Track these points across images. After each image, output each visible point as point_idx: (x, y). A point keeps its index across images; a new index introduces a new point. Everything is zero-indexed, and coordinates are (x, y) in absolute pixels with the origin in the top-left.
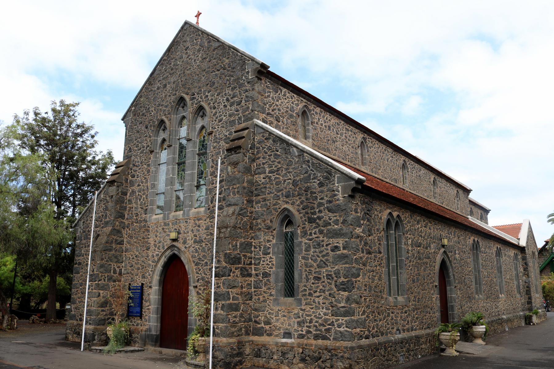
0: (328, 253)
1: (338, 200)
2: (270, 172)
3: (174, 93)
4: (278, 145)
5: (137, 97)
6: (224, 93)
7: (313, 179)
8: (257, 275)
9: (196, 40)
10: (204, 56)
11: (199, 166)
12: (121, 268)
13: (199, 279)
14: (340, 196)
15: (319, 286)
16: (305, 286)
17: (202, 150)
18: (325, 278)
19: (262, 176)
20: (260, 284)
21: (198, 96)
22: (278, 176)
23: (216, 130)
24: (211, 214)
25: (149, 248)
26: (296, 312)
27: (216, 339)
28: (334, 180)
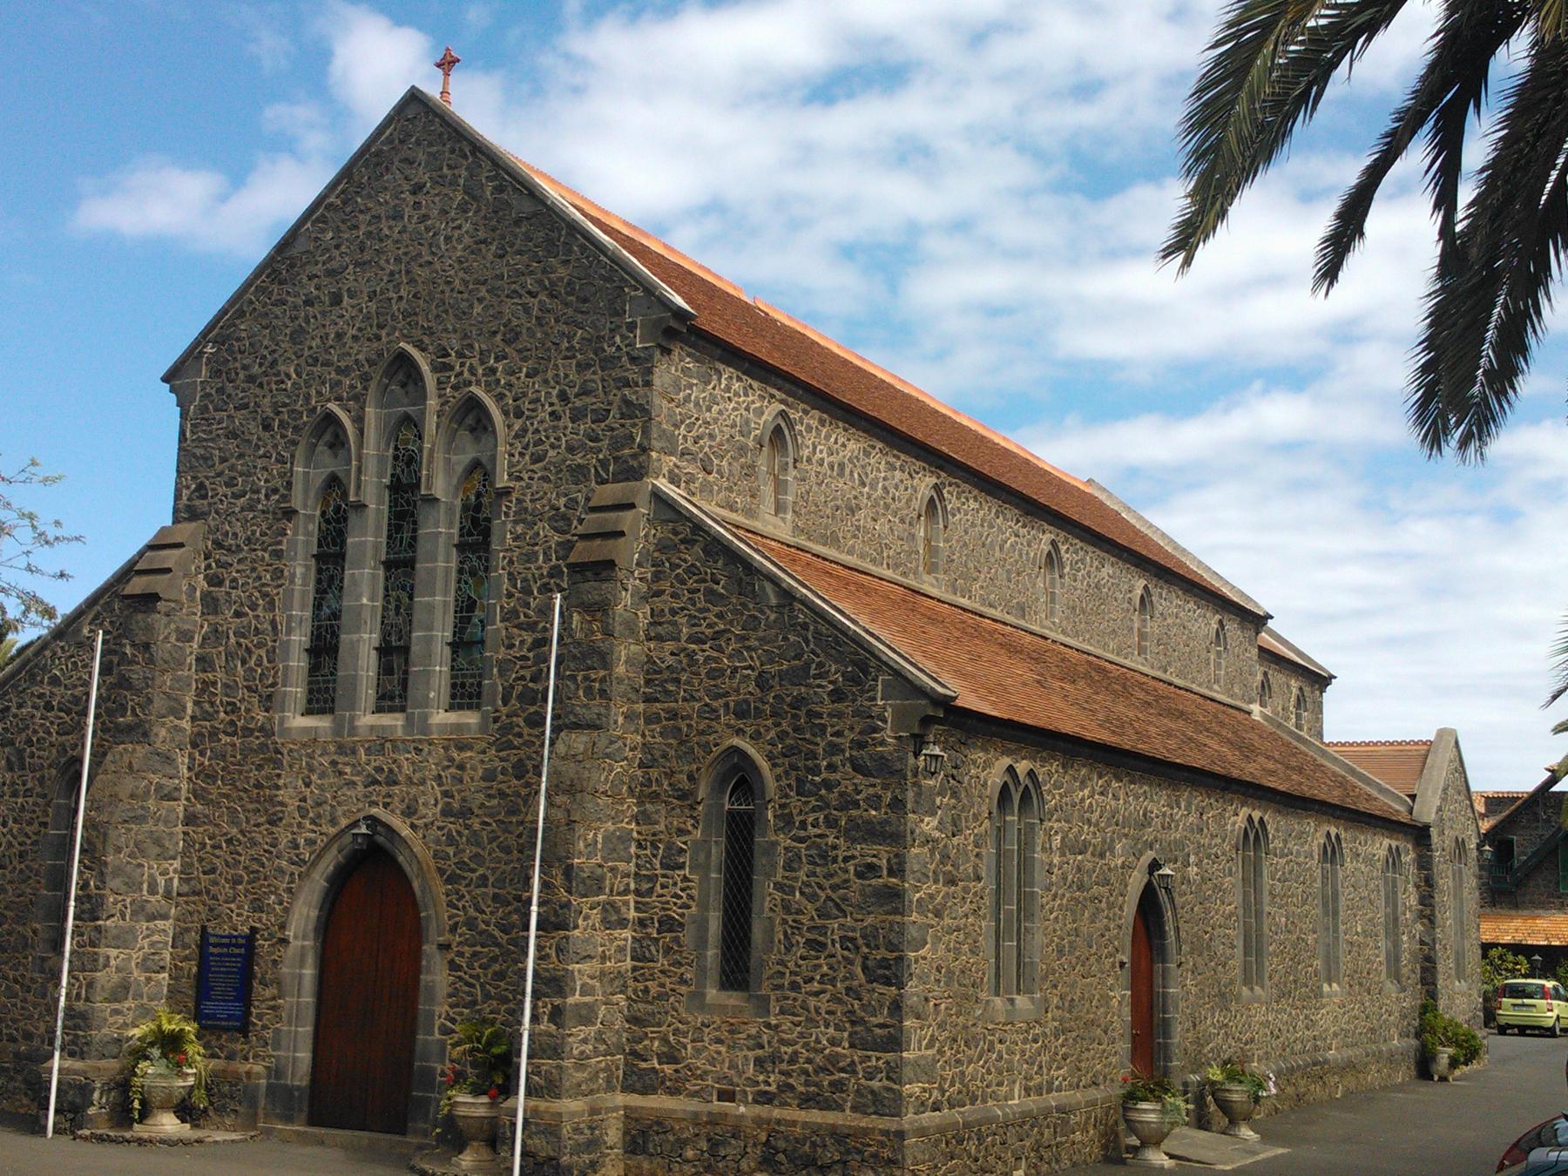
0: (847, 881)
1: (883, 743)
2: (691, 639)
3: (370, 332)
4: (720, 563)
5: (223, 312)
6: (550, 374)
7: (815, 677)
8: (642, 923)
9: (450, 167)
10: (482, 235)
11: (459, 582)
12: (172, 875)
13: (457, 923)
14: (888, 734)
15: (820, 966)
16: (782, 963)
17: (470, 534)
18: (838, 945)
19: (670, 646)
20: (653, 948)
21: (462, 365)
22: (715, 654)
23: (523, 484)
24: (502, 736)
25: (281, 819)
26: (753, 1031)
27: (533, 1103)
28: (873, 688)
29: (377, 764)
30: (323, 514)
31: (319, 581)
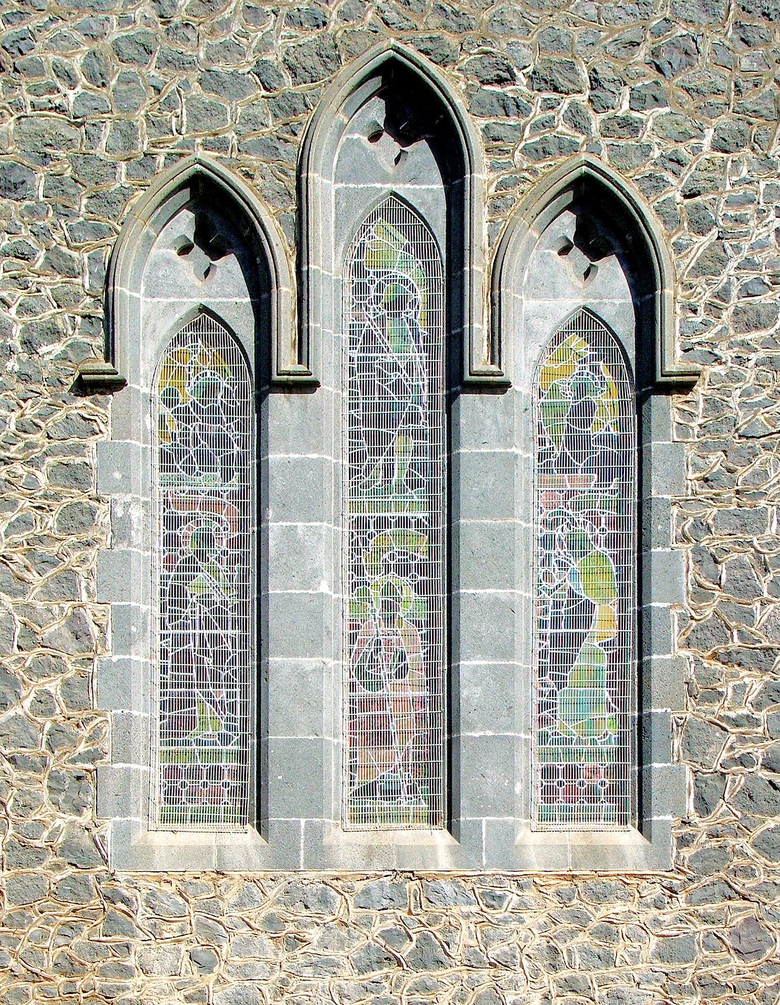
29: (390, 924)
30: (170, 399)
31: (171, 541)
